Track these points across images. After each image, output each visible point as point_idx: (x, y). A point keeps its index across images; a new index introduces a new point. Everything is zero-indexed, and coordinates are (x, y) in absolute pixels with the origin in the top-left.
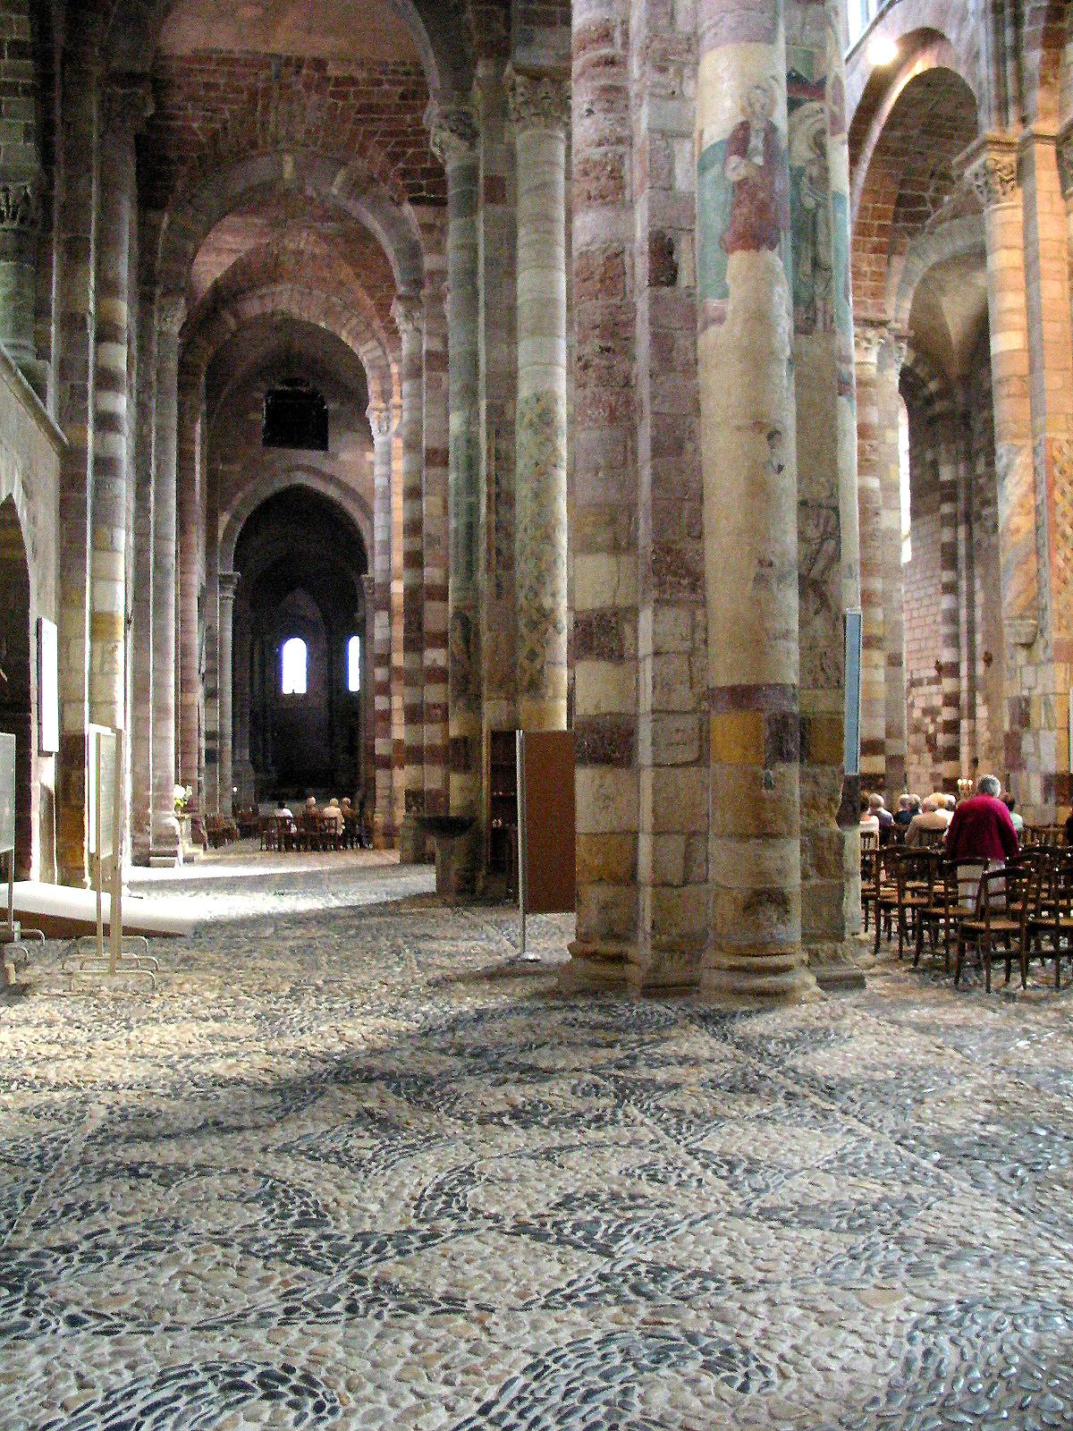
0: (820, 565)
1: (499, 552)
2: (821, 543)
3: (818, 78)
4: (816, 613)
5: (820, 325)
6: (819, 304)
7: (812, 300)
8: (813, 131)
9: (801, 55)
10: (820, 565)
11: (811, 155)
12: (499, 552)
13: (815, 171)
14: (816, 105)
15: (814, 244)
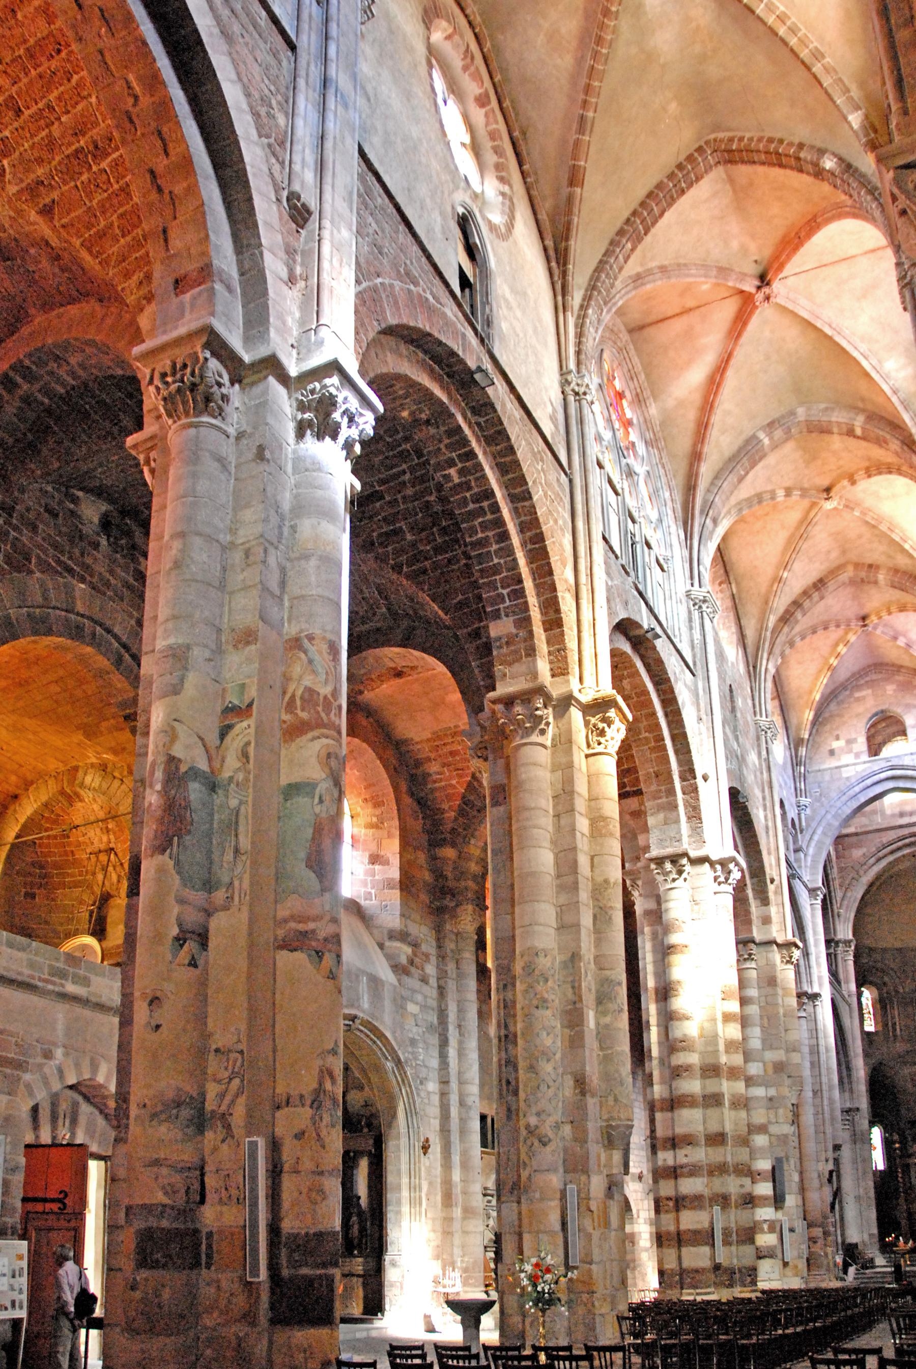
0: (226, 1101)
1: (508, 1082)
2: (229, 1083)
3: (247, 702)
4: (223, 1141)
5: (236, 899)
6: (236, 883)
7: (231, 883)
8: (242, 744)
9: (237, 688)
10: (226, 1101)
11: (239, 765)
12: (508, 1082)
13: (240, 776)
14: (245, 724)
15: (236, 836)
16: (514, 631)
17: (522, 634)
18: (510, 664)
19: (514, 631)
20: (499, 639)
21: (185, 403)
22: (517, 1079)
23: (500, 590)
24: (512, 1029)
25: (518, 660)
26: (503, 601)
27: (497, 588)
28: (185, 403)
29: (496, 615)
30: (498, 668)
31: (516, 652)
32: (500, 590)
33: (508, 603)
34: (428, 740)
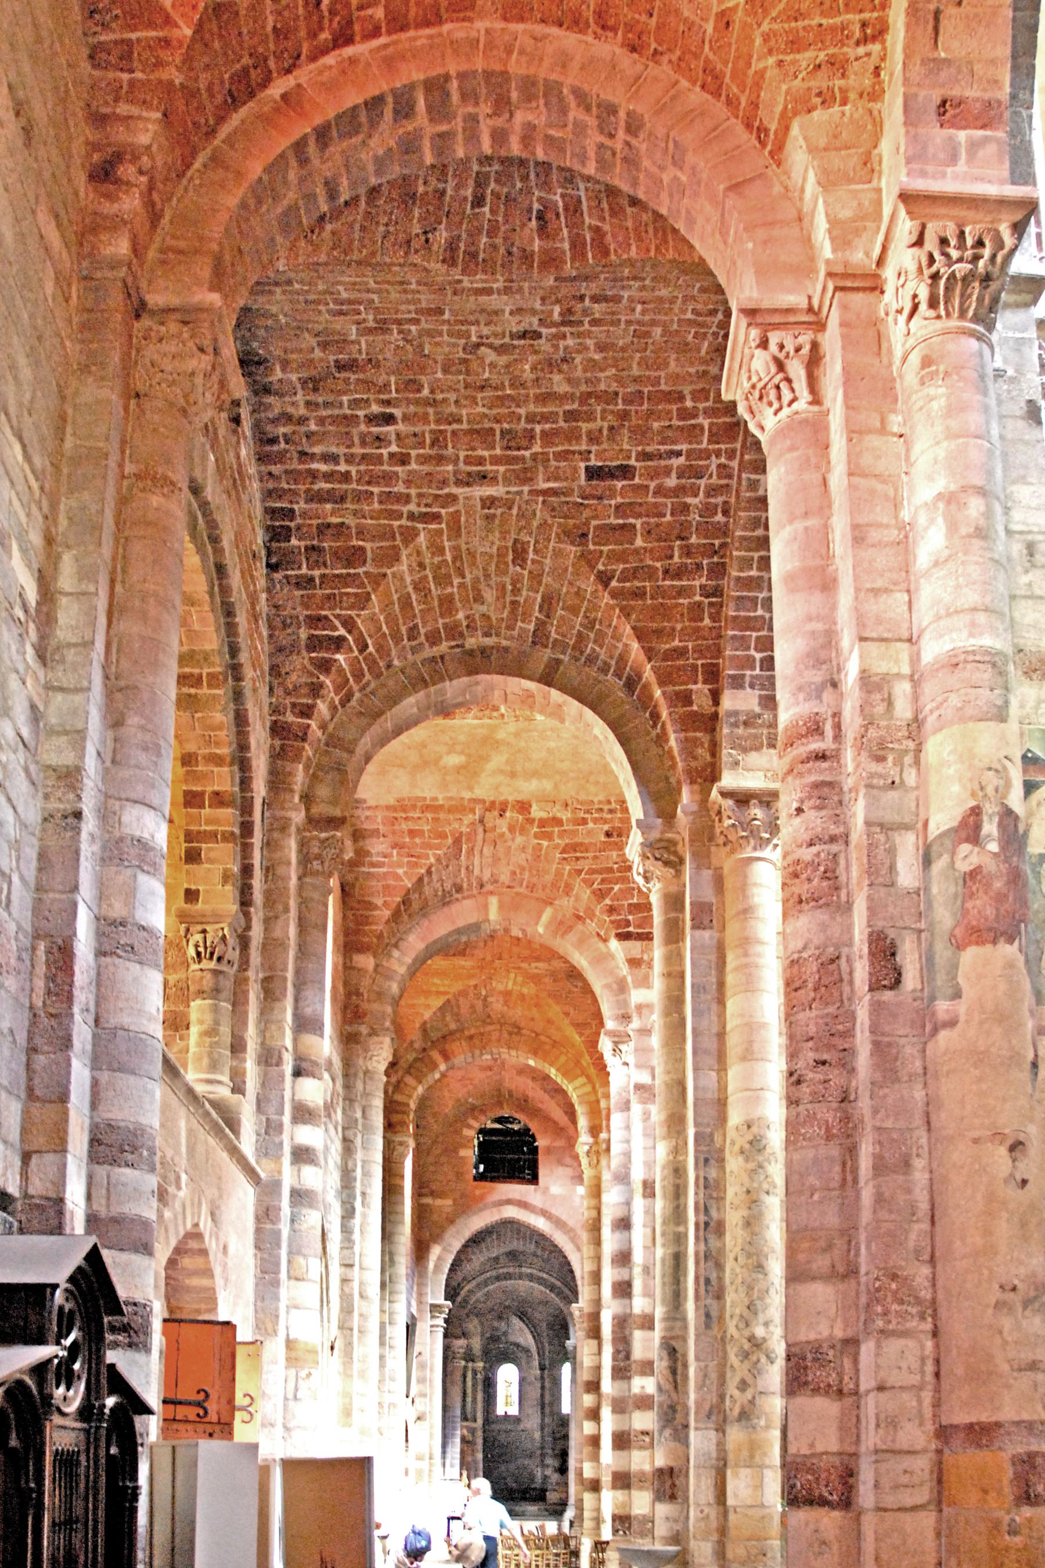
16: (757, 709)
17: (767, 716)
18: (745, 750)
19: (757, 709)
20: (736, 713)
21: (964, 297)
22: (720, 1279)
23: (752, 652)
24: (714, 1214)
25: (758, 748)
26: (753, 668)
27: (748, 648)
28: (964, 297)
29: (738, 683)
30: (727, 753)
31: (756, 737)
32: (752, 652)
33: (757, 671)
34: (388, 808)
